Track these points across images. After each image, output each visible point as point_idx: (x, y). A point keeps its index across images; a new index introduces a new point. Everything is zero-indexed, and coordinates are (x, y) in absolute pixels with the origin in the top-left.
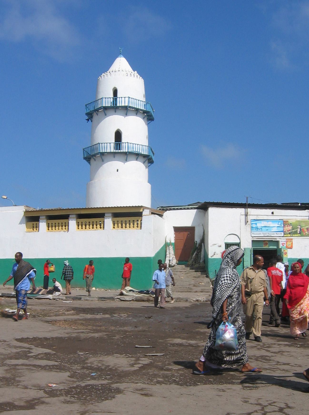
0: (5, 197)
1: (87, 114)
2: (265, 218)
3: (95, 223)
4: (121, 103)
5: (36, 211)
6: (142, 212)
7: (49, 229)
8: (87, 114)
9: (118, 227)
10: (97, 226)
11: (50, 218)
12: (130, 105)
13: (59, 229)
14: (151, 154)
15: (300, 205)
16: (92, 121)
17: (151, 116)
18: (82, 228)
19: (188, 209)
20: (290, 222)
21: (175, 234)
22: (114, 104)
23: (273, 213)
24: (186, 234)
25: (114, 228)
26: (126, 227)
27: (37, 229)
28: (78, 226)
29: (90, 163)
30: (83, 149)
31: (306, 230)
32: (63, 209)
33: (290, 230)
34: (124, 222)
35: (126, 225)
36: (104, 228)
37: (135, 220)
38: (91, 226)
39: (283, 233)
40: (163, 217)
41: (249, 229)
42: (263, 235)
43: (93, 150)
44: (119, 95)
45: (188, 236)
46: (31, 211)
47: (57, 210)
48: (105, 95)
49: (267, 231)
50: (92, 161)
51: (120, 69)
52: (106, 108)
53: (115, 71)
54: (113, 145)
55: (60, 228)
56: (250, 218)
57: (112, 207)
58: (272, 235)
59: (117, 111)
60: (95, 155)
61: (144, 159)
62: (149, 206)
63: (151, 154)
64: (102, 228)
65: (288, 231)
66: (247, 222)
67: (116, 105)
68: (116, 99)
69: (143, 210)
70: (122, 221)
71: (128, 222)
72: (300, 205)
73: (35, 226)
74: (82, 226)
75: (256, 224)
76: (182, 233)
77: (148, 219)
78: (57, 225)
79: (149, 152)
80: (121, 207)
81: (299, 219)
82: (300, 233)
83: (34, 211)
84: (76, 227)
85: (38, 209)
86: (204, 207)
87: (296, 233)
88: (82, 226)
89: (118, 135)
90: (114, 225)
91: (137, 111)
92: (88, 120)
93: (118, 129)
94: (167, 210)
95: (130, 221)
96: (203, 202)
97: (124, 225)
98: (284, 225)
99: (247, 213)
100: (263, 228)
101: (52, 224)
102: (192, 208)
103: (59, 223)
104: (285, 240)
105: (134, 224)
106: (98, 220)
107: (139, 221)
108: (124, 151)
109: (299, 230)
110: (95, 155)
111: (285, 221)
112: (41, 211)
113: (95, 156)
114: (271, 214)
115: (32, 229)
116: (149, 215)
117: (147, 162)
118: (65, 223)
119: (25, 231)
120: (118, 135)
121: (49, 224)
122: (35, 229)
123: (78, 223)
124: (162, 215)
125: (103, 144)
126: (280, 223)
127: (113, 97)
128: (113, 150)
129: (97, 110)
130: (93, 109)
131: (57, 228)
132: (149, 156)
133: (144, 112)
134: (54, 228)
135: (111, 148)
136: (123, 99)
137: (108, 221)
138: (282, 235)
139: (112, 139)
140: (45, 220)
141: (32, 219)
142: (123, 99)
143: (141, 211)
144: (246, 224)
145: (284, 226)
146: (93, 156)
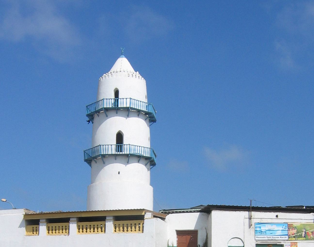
0: (5, 200)
1: (88, 115)
2: (269, 221)
3: (96, 227)
4: (122, 104)
5: (36, 214)
6: (144, 215)
7: (49, 233)
8: (88, 115)
9: (120, 230)
10: (98, 229)
11: (50, 221)
12: (132, 107)
13: (59, 233)
14: (153, 156)
15: (304, 208)
16: (93, 123)
17: (153, 117)
18: (83, 232)
19: (191, 212)
20: (295, 225)
21: (177, 237)
22: (115, 105)
23: (277, 216)
24: (189, 237)
25: (115, 231)
26: (127, 231)
27: (37, 232)
28: (79, 229)
29: (90, 165)
30: (84, 151)
31: (310, 234)
32: (64, 212)
33: (294, 234)
34: (125, 225)
35: (127, 228)
36: (105, 231)
37: (137, 224)
38: (92, 229)
39: (287, 237)
40: (166, 220)
41: (253, 233)
42: (267, 239)
43: (94, 152)
44: (120, 96)
45: (190, 240)
46: (31, 214)
47: (58, 213)
48: (106, 96)
49: (272, 235)
50: (93, 163)
51: (121, 70)
52: (107, 110)
53: (117, 72)
54: (114, 147)
55: (61, 231)
56: (254, 221)
57: (113, 210)
58: (277, 239)
59: (119, 112)
60: (95, 158)
61: (145, 162)
62: (151, 209)
63: (153, 156)
64: (103, 232)
65: (293, 235)
66: (251, 225)
67: (117, 106)
68: (118, 100)
69: (145, 213)
70: (123, 225)
71: (129, 225)
72: (304, 208)
73: (35, 229)
74: (83, 230)
75: (260, 227)
76: (184, 237)
77: (150, 222)
78: (57, 228)
79: (151, 154)
80: (122, 210)
81: (304, 222)
82: (305, 237)
83: (34, 214)
84: (77, 230)
85: (38, 212)
86: (207, 211)
87: (300, 236)
88: (83, 230)
89: (120, 137)
90: (115, 229)
91: (139, 112)
92: (89, 121)
93: (120, 131)
94: (169, 213)
95: (131, 224)
96: (206, 205)
97: (125, 228)
98: (288, 228)
99: (251, 216)
100: (267, 232)
101: (52, 227)
102: (194, 212)
103: (59, 227)
104: (290, 244)
105: (135, 228)
106: (99, 223)
107: (141, 224)
108: (126, 153)
109: (304, 233)
110: (95, 158)
111: (289, 225)
112: (41, 214)
113: (96, 158)
114: (275, 217)
115: (32, 233)
116: (151, 218)
117: (149, 164)
118: (66, 226)
119: (25, 234)
120: (120, 137)
121: (49, 227)
122: (35, 233)
123: (79, 226)
124: (165, 219)
125: (104, 146)
126: (284, 227)
127: (115, 144)
128: (114, 152)
129: (98, 112)
130: (94, 111)
131: (57, 231)
132: (151, 158)
133: (146, 113)
134: (54, 231)
135: (112, 150)
136: (125, 100)
137: (110, 225)
138: (287, 239)
139: (114, 141)
140: (45, 224)
141: (32, 223)
142: (125, 100)
143: (143, 214)
144: (250, 227)
145: (289, 229)
146: (94, 158)
